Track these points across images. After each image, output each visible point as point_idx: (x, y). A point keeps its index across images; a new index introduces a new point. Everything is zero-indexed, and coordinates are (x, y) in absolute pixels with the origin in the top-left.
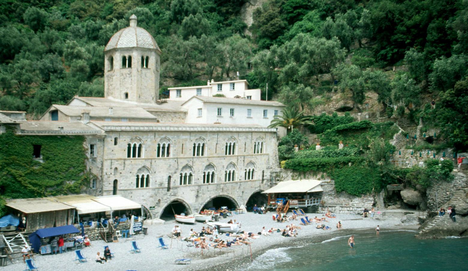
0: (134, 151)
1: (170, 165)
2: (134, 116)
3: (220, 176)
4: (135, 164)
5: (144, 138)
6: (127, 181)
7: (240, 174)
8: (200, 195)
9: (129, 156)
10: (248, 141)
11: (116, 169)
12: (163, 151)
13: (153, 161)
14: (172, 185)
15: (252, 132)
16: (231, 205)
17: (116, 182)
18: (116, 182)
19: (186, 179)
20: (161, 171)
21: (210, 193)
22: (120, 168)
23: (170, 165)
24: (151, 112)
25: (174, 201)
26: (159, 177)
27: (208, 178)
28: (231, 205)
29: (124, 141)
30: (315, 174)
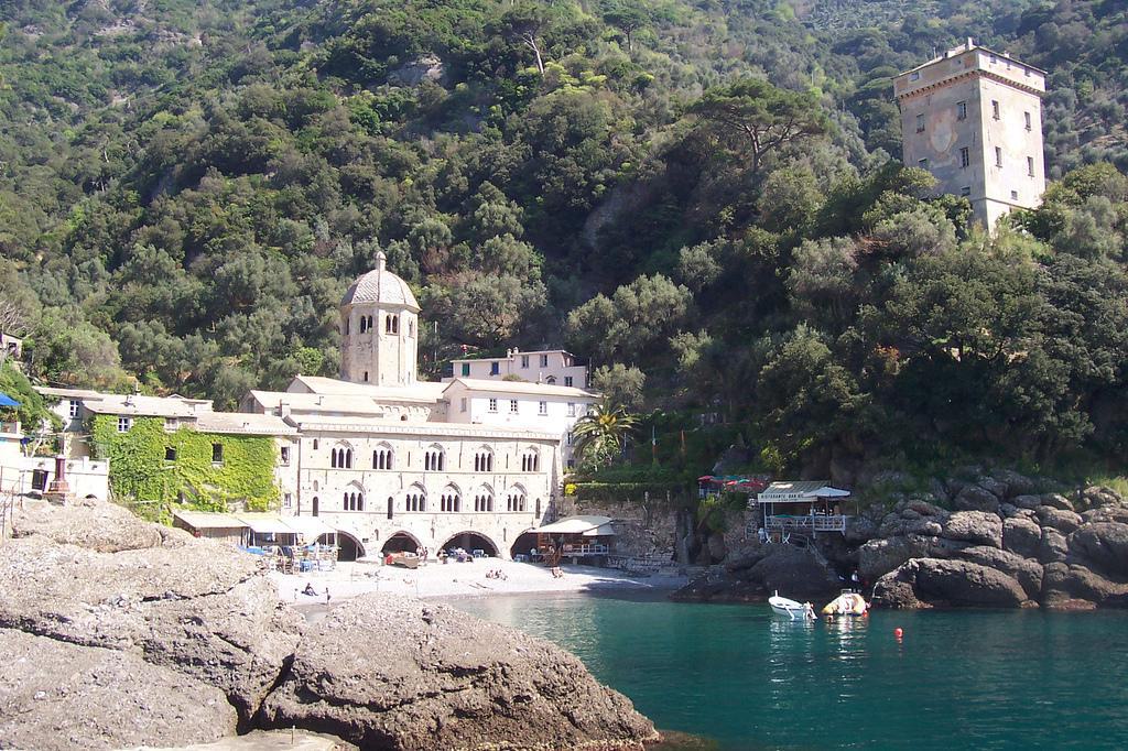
0: (342, 460)
1: (391, 483)
2: (352, 410)
3: (467, 503)
4: (341, 481)
5: (353, 441)
6: (331, 500)
7: (500, 502)
8: (436, 528)
9: (334, 465)
10: (512, 454)
11: (316, 482)
12: (382, 461)
13: (366, 474)
14: (395, 510)
15: (518, 439)
16: (489, 549)
17: (315, 500)
18: (315, 500)
19: (417, 504)
20: (380, 487)
21: (453, 525)
22: (321, 483)
23: (391, 483)
24: (379, 402)
25: (398, 534)
26: (375, 499)
27: (451, 504)
28: (489, 549)
29: (328, 445)
30: (605, 506)
